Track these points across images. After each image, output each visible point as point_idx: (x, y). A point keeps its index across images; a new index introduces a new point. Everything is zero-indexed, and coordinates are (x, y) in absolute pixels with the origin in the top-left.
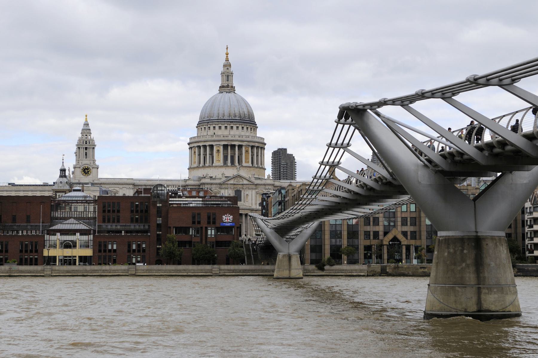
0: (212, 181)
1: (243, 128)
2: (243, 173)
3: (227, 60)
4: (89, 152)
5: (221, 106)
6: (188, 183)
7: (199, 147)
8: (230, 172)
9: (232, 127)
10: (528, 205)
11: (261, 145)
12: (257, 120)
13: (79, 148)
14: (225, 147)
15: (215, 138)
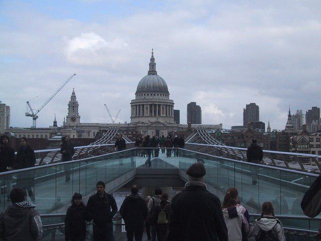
0: (143, 125)
1: (161, 95)
2: (162, 121)
3: (152, 56)
4: (76, 108)
5: (149, 83)
6: (131, 125)
7: (136, 106)
8: (153, 120)
9: (155, 95)
10: (291, 144)
11: (171, 104)
12: (170, 89)
13: (69, 107)
14: (151, 105)
15: (145, 100)
